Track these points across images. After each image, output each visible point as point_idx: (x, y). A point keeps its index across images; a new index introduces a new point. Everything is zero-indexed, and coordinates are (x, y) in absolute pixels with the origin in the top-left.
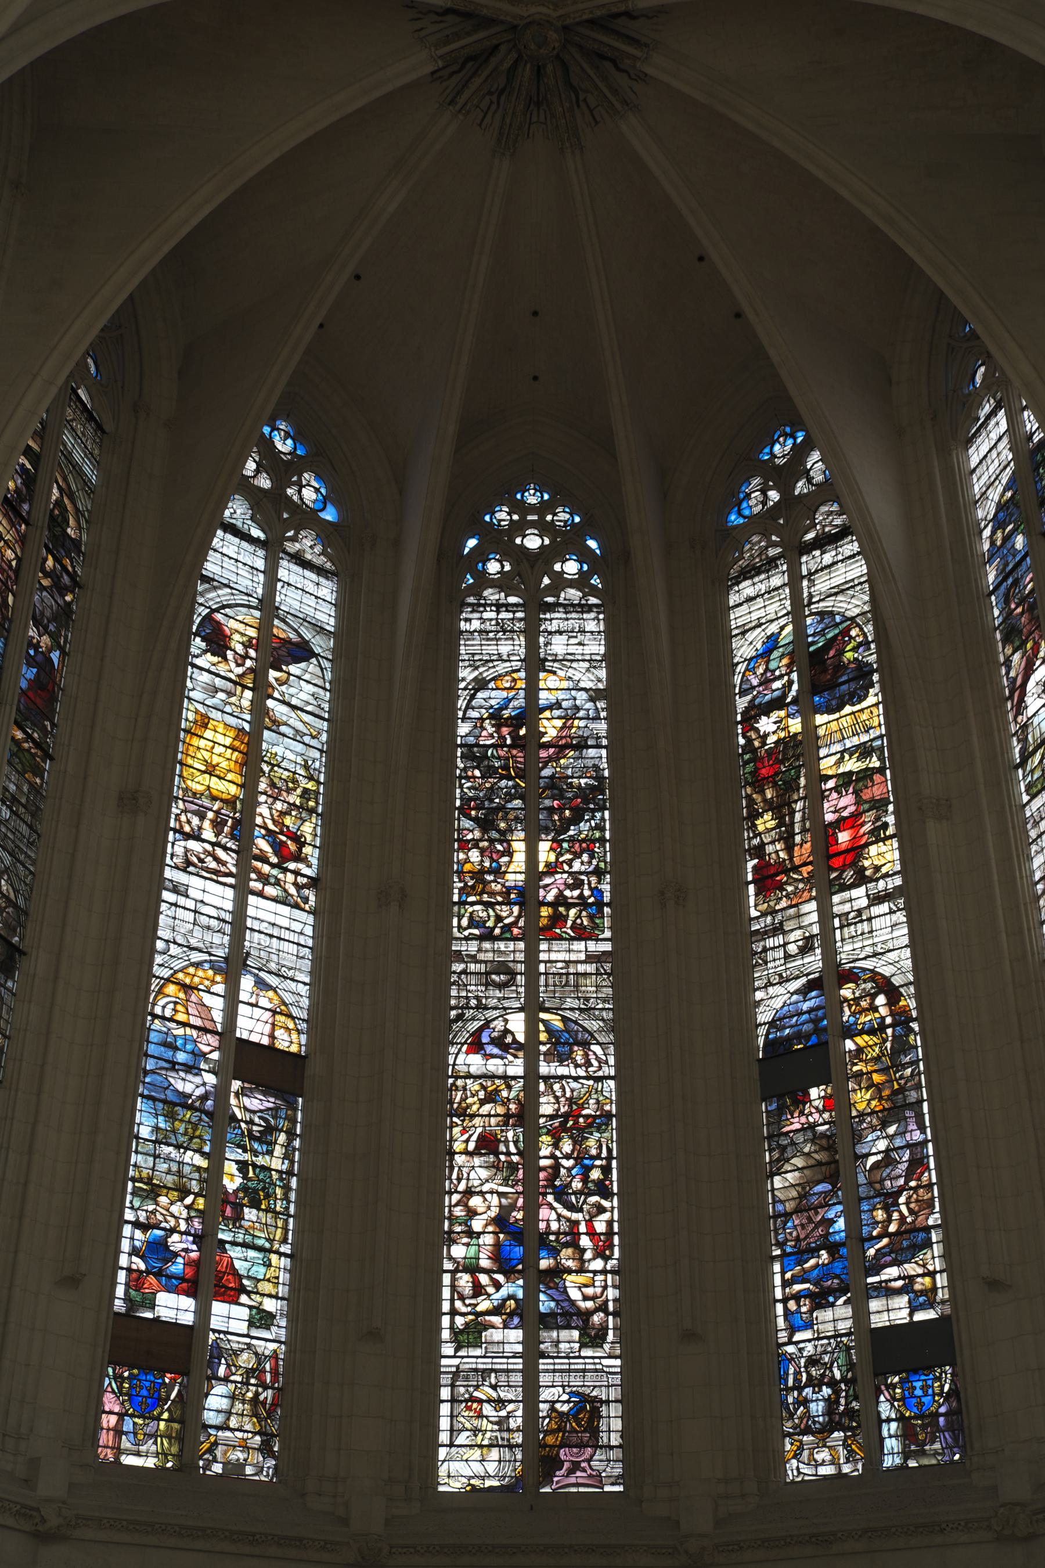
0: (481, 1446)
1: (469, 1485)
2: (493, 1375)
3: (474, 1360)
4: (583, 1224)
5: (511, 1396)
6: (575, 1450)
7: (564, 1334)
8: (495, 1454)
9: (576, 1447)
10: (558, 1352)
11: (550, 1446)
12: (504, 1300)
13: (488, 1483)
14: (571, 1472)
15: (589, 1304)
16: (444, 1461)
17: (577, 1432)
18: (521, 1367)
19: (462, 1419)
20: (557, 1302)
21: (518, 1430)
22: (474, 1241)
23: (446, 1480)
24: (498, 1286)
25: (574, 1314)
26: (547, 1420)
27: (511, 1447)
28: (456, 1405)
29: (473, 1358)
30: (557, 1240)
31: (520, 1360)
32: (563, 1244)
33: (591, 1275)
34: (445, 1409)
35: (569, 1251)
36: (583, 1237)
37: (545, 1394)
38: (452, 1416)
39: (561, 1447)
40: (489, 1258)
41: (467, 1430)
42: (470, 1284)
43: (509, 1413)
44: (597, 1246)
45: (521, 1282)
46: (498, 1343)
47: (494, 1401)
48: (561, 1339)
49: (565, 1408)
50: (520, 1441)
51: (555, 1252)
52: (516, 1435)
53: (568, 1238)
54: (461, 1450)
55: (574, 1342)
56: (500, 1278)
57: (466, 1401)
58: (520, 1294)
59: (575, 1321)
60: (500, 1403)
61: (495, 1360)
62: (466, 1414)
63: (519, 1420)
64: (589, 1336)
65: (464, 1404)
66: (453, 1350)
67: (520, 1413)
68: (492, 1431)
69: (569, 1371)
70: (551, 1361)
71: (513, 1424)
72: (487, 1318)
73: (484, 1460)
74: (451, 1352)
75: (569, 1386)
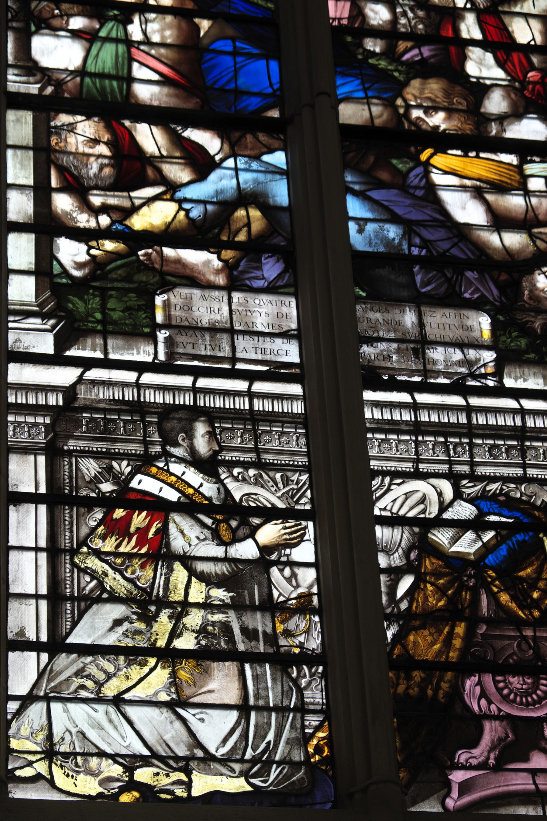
0: (169, 656)
1: (131, 785)
2: (201, 429)
3: (130, 376)
4: (470, 19)
5: (269, 497)
6: (516, 681)
7: (439, 321)
8: (222, 684)
9: (518, 670)
10: (425, 373)
11: (427, 666)
12: (226, 206)
13: (203, 784)
14: (510, 753)
15: (514, 240)
16: (27, 700)
17: (519, 624)
18: (298, 408)
19: (94, 563)
20: (409, 228)
21: (303, 606)
22: (109, 29)
23: (41, 767)
24: (202, 164)
25: (470, 265)
26: (406, 583)
27: (283, 661)
28: (67, 514)
29: (125, 370)
30: (390, 53)
31: (296, 389)
32: (410, 64)
33: (511, 159)
34: (27, 526)
35: (434, 87)
36: (475, 53)
37: (392, 499)
38: (54, 551)
39: (468, 666)
40: (165, 81)
41: (114, 598)
42: (102, 149)
43: (265, 550)
44: (524, 82)
45: (279, 159)
46: (213, 330)
47: (209, 508)
48: (432, 332)
49: (467, 545)
50: (314, 643)
51: (385, 85)
52: (298, 623)
53: (426, 51)
54: (97, 666)
55: (479, 346)
56: (209, 141)
57: (107, 503)
58: (280, 192)
59: (472, 284)
60: (231, 518)
61: (202, 383)
62: (108, 546)
63: (308, 576)
64: (526, 330)
65: (99, 515)
66: (50, 338)
67: (305, 552)
68: (207, 606)
69: (470, 431)
70: (404, 397)
71: (281, 586)
72: (168, 252)
73: (186, 704)
74: (46, 345)
75: (474, 478)
